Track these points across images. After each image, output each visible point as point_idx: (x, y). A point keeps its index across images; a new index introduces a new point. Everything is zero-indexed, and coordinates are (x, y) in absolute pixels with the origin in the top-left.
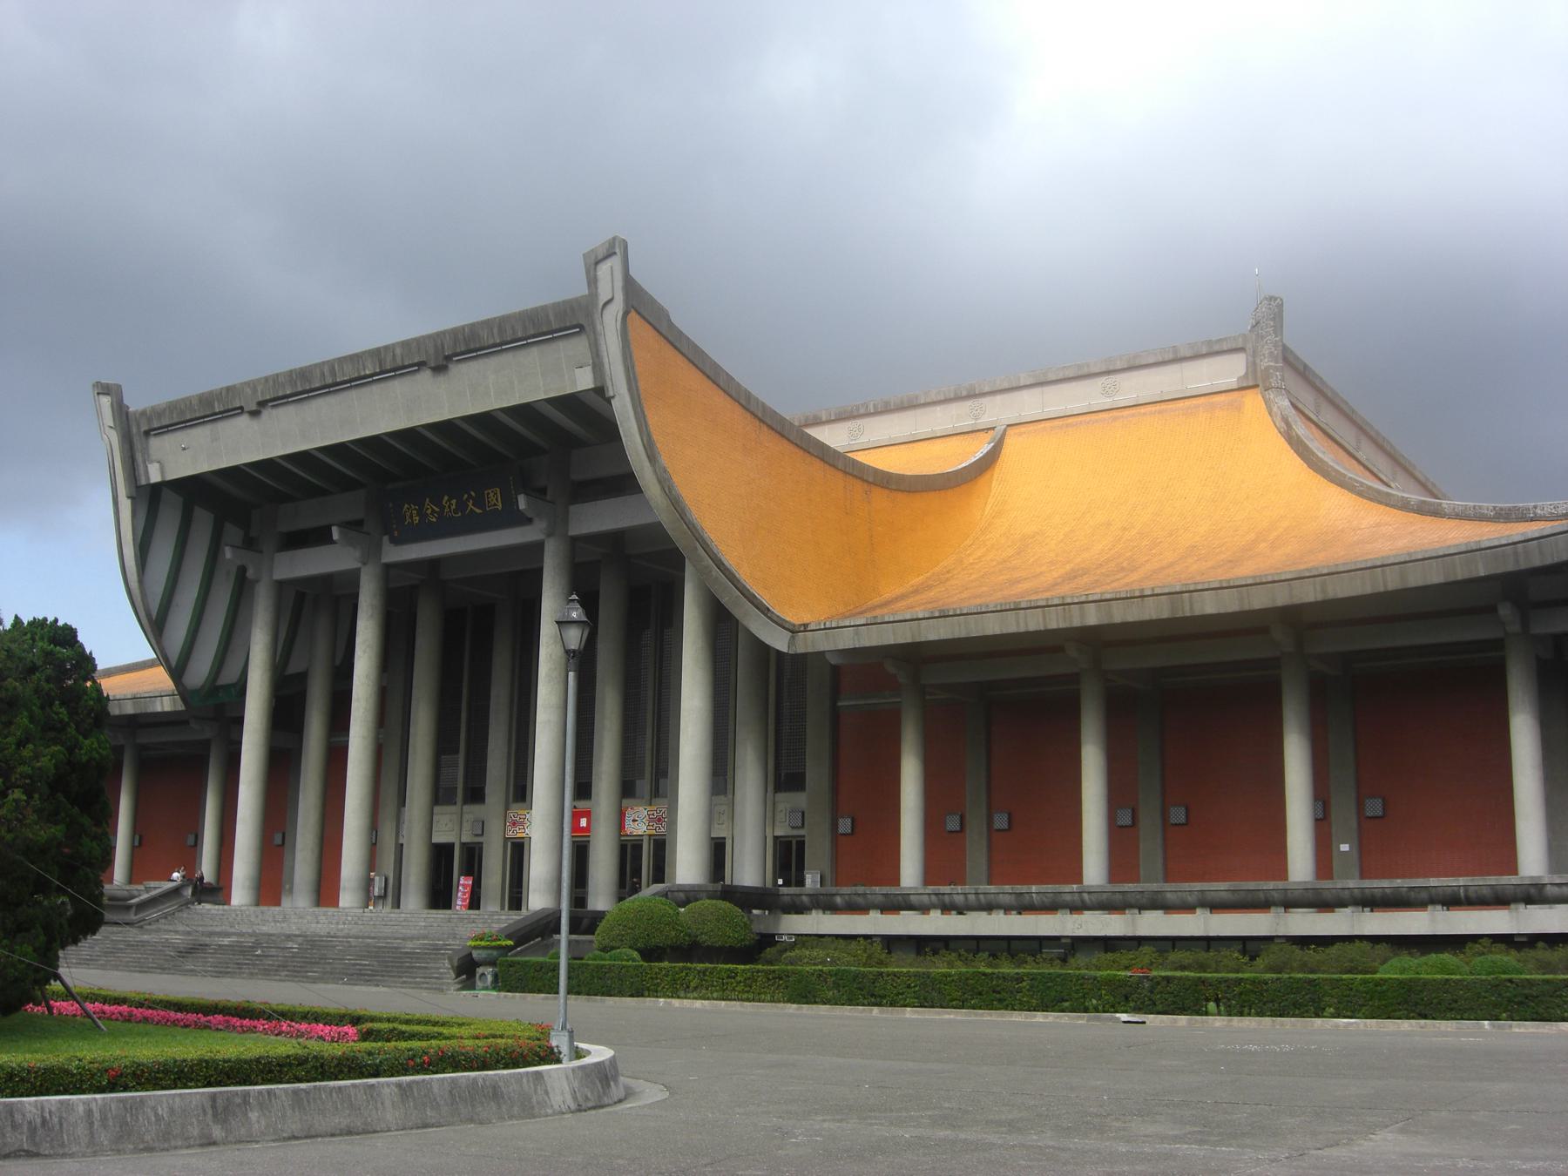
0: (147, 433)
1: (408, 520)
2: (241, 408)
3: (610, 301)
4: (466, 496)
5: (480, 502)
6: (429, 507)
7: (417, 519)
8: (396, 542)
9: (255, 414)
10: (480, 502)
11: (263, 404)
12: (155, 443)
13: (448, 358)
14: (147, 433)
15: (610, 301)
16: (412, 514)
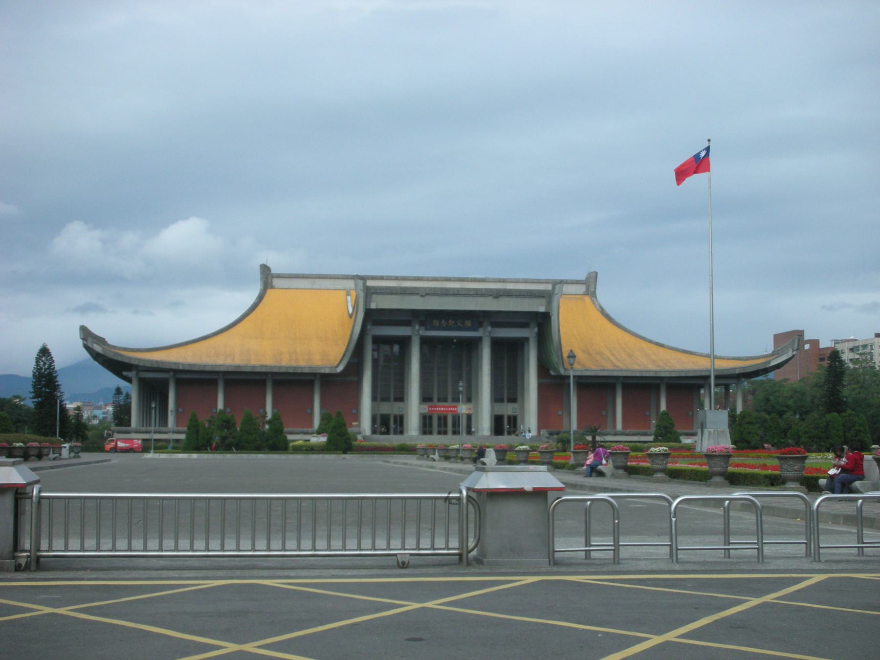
0: (373, 293)
1: (434, 324)
2: (418, 294)
3: (557, 294)
4: (458, 321)
5: (463, 323)
6: (443, 322)
7: (438, 325)
8: (426, 329)
9: (422, 296)
10: (463, 323)
11: (427, 294)
12: (374, 296)
13: (500, 296)
14: (373, 293)
15: (557, 294)
16: (436, 323)
